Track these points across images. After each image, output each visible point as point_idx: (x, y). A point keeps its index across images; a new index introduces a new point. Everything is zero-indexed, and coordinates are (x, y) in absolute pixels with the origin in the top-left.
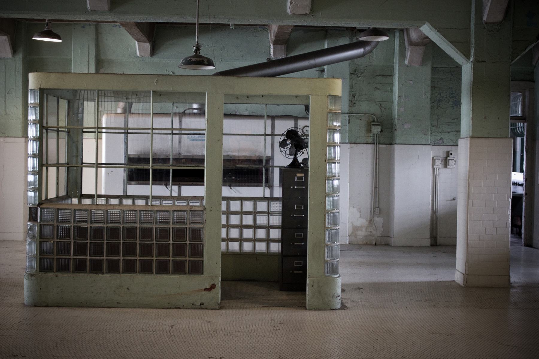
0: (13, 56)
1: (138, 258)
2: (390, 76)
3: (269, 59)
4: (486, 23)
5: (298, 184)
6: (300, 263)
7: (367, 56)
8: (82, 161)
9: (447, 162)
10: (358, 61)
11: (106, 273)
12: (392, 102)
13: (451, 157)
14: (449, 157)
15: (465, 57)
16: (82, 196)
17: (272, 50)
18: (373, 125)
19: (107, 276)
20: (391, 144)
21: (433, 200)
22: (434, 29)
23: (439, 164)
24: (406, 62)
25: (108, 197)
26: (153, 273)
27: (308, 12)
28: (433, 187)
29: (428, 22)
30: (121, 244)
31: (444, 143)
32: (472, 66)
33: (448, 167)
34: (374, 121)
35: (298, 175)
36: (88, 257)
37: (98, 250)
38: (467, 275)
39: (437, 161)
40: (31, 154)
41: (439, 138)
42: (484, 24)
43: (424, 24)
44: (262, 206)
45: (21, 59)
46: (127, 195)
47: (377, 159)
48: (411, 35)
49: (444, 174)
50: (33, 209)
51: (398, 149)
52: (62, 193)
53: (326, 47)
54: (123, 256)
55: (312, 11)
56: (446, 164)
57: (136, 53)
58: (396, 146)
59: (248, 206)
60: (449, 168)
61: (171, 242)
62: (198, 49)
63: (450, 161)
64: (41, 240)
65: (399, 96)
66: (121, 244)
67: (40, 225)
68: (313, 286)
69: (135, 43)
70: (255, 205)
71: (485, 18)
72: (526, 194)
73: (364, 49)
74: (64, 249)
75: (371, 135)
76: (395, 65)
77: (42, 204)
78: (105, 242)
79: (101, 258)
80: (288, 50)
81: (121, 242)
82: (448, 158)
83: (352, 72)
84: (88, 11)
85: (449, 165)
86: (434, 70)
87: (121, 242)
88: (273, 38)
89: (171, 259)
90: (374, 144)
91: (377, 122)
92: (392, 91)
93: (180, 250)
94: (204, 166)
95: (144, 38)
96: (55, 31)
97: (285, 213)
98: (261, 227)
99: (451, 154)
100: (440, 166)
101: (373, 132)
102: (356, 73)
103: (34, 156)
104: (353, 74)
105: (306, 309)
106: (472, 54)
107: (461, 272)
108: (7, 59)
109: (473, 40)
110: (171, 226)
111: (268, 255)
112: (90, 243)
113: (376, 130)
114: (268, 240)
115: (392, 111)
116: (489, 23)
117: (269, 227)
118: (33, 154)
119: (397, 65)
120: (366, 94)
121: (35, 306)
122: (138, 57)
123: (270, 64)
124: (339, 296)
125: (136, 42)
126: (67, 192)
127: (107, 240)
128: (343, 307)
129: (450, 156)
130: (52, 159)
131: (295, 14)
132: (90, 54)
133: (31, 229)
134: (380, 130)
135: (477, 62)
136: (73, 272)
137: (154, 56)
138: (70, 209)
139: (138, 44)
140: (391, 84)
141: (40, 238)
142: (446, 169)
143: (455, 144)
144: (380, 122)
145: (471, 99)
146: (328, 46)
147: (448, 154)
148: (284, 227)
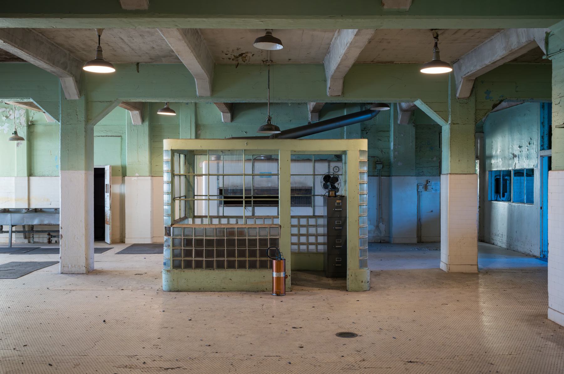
0: (142, 124)
1: (237, 259)
2: (388, 131)
3: (309, 123)
4: (458, 99)
5: (337, 207)
6: (340, 259)
7: (373, 119)
8: (194, 194)
9: (426, 187)
10: (366, 122)
11: (216, 269)
13: (429, 184)
14: (428, 184)
15: (445, 121)
16: (194, 217)
17: (310, 116)
18: (377, 164)
20: (389, 176)
21: (418, 212)
22: (423, 103)
23: (421, 187)
24: (399, 122)
25: (212, 217)
27: (340, 94)
28: (418, 204)
29: (419, 98)
30: (226, 250)
31: (424, 174)
32: (450, 127)
33: (427, 190)
34: (378, 162)
35: (337, 201)
36: (204, 259)
37: (210, 254)
38: (450, 265)
39: (420, 186)
40: (166, 192)
41: (421, 171)
42: (457, 99)
43: (417, 100)
44: (312, 222)
45: (148, 126)
46: (223, 216)
47: (381, 186)
50: (167, 228)
51: (394, 180)
52: (183, 215)
53: (345, 114)
55: (343, 93)
56: (426, 188)
57: (221, 120)
58: (393, 177)
59: (303, 222)
60: (428, 191)
61: (258, 248)
62: (269, 120)
63: (429, 186)
64: (174, 248)
66: (226, 250)
67: (173, 238)
68: (351, 275)
69: (221, 114)
70: (308, 221)
71: (458, 95)
73: (371, 114)
74: (188, 253)
75: (376, 170)
76: (391, 124)
78: (215, 249)
79: (213, 259)
80: (320, 117)
81: (226, 248)
82: (427, 185)
83: (362, 130)
84: (197, 97)
85: (428, 189)
87: (226, 248)
88: (311, 109)
89: (258, 259)
90: (378, 176)
91: (380, 162)
92: (389, 141)
93: (263, 253)
94: (278, 197)
95: (227, 111)
96: (171, 107)
97: (330, 225)
98: (312, 235)
99: (429, 182)
100: (423, 190)
101: (377, 169)
102: (365, 130)
103: (168, 193)
104: (363, 130)
106: (450, 119)
107: (445, 263)
108: (138, 126)
110: (258, 238)
111: (317, 253)
112: (205, 249)
113: (379, 167)
114: (317, 244)
115: (389, 154)
116: (460, 98)
117: (317, 236)
118: (167, 192)
119: (393, 125)
120: (372, 144)
121: (170, 291)
122: (223, 122)
123: (310, 126)
124: (368, 282)
125: (222, 113)
126: (185, 215)
127: (216, 248)
129: (429, 183)
130: (177, 195)
131: (332, 96)
132: (192, 121)
134: (382, 167)
135: (453, 124)
136: (194, 269)
137: (233, 122)
138: (192, 228)
139: (223, 114)
140: (389, 137)
141: (173, 246)
143: (432, 175)
144: (382, 162)
145: (449, 149)
146: (346, 113)
147: (428, 182)
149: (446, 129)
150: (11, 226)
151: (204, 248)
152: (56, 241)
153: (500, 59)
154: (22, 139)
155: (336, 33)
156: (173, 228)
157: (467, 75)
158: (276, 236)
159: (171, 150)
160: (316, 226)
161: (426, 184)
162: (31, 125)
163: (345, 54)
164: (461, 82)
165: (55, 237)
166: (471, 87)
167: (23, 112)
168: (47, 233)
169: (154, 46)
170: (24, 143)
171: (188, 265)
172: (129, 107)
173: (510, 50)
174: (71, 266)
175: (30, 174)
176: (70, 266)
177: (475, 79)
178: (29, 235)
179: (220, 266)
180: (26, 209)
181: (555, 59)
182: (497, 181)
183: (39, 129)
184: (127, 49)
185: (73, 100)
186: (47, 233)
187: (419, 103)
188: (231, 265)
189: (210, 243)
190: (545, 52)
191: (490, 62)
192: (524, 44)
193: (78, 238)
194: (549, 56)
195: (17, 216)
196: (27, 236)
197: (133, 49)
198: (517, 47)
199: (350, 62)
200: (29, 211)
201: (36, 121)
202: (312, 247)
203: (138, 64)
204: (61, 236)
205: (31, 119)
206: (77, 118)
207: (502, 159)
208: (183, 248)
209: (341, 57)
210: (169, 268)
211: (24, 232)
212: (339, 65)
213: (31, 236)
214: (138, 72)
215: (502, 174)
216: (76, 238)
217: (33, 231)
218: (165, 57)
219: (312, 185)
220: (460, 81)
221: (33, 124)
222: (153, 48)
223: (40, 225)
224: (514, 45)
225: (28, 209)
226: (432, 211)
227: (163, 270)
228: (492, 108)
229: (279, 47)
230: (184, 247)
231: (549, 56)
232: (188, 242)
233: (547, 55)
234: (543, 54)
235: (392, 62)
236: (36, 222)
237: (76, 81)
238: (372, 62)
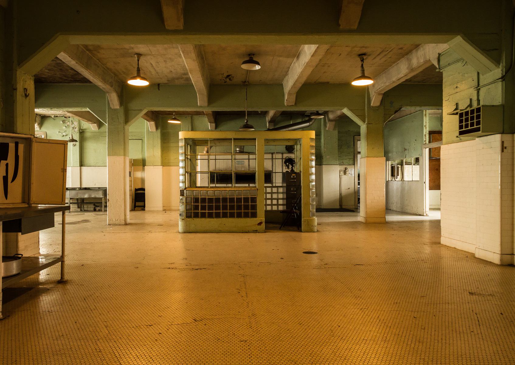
2: (319, 135)
4: (372, 107)
11: (215, 218)
12: (321, 147)
13: (347, 170)
19: (215, 219)
22: (349, 110)
23: (342, 173)
24: (327, 129)
26: (235, 217)
27: (294, 104)
35: (293, 175)
36: (207, 211)
37: (210, 208)
48: (330, 117)
49: (344, 177)
50: (182, 191)
54: (222, 210)
55: (296, 104)
56: (345, 173)
61: (243, 204)
62: (247, 122)
65: (324, 144)
71: (372, 105)
73: (309, 123)
74: (196, 208)
77: (186, 188)
78: (214, 204)
86: (339, 132)
87: (221, 204)
92: (320, 142)
93: (246, 207)
105: (302, 232)
106: (366, 121)
109: (366, 114)
117: (278, 199)
121: (184, 233)
128: (318, 231)
131: (288, 105)
133: (182, 199)
135: (368, 124)
138: (199, 191)
141: (186, 203)
142: (345, 176)
147: (346, 169)
148: (287, 199)
149: (363, 128)
150: (70, 199)
151: (207, 204)
152: (99, 209)
153: (404, 76)
154: (76, 141)
155: (295, 59)
156: (186, 190)
157: (379, 90)
158: (255, 196)
159: (185, 138)
160: (278, 193)
161: (345, 171)
162: (82, 132)
163: (301, 72)
164: (374, 95)
165: (98, 206)
166: (381, 99)
167: (76, 124)
168: (93, 204)
169: (172, 70)
170: (78, 144)
171: (196, 216)
172: (148, 119)
174: (115, 220)
175: (82, 164)
176: (114, 220)
177: (383, 93)
178: (81, 206)
179: (218, 216)
180: (79, 188)
181: (444, 70)
183: (87, 135)
184: (153, 72)
185: (116, 109)
186: (93, 204)
187: (346, 111)
188: (225, 216)
189: (210, 200)
191: (396, 79)
193: (119, 201)
194: (441, 69)
195: (73, 192)
196: (80, 206)
197: (157, 73)
199: (303, 80)
200: (80, 189)
201: (85, 129)
202: (275, 208)
203: (159, 84)
204: (108, 200)
205: (82, 128)
206: (119, 121)
208: (193, 204)
209: (298, 75)
210: (183, 218)
211: (77, 203)
212: (296, 81)
213: (82, 206)
214: (159, 90)
216: (118, 202)
217: (84, 202)
218: (178, 79)
219: (271, 170)
220: (374, 94)
221: (83, 132)
222: (171, 71)
223: (89, 198)
225: (81, 188)
226: (349, 189)
227: (179, 219)
229: (258, 67)
230: (193, 203)
231: (441, 69)
232: (196, 200)
233: (439, 68)
234: (436, 68)
235: (328, 83)
236: (86, 196)
237: (118, 96)
238: (315, 82)
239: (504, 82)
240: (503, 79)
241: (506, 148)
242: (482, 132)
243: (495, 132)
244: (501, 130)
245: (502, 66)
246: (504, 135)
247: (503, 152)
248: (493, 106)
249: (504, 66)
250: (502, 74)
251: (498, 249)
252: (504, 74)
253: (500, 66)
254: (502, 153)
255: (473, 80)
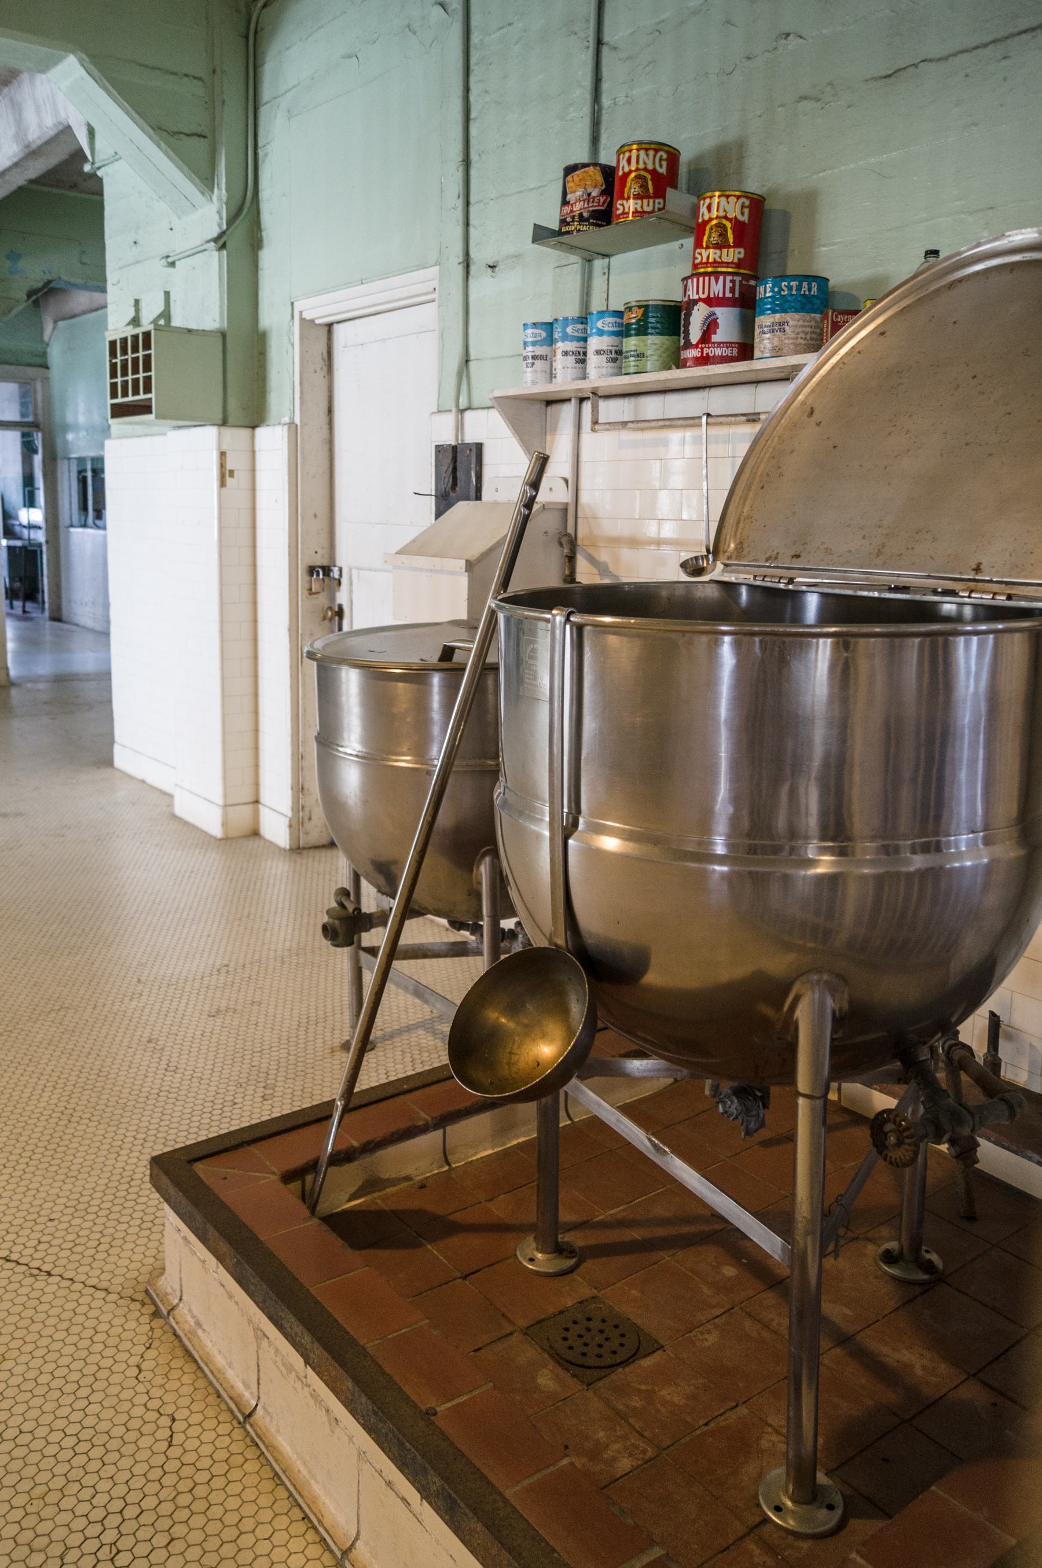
72: (47, 542)
173: (26, 142)
182: (83, 481)
190: (90, 158)
192: (52, 133)
198: (39, 138)
207: (87, 431)
215: (89, 467)
224: (31, 130)
228: (26, 298)
234: (86, 159)
239: (225, 252)
240: (221, 243)
241: (231, 473)
242: (157, 417)
243: (201, 421)
244: (219, 416)
245: (220, 199)
246: (223, 429)
247: (225, 486)
248: (190, 331)
249: (224, 199)
250: (220, 225)
251: (216, 793)
252: (225, 227)
253: (215, 198)
254: (224, 489)
255: (171, 229)
